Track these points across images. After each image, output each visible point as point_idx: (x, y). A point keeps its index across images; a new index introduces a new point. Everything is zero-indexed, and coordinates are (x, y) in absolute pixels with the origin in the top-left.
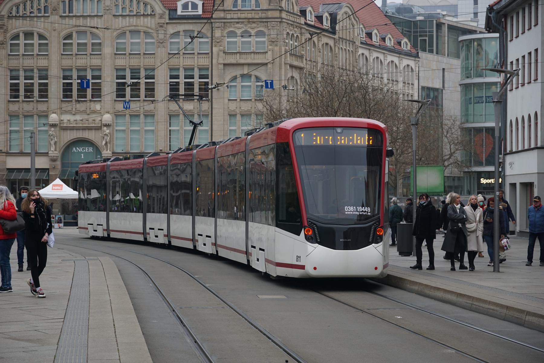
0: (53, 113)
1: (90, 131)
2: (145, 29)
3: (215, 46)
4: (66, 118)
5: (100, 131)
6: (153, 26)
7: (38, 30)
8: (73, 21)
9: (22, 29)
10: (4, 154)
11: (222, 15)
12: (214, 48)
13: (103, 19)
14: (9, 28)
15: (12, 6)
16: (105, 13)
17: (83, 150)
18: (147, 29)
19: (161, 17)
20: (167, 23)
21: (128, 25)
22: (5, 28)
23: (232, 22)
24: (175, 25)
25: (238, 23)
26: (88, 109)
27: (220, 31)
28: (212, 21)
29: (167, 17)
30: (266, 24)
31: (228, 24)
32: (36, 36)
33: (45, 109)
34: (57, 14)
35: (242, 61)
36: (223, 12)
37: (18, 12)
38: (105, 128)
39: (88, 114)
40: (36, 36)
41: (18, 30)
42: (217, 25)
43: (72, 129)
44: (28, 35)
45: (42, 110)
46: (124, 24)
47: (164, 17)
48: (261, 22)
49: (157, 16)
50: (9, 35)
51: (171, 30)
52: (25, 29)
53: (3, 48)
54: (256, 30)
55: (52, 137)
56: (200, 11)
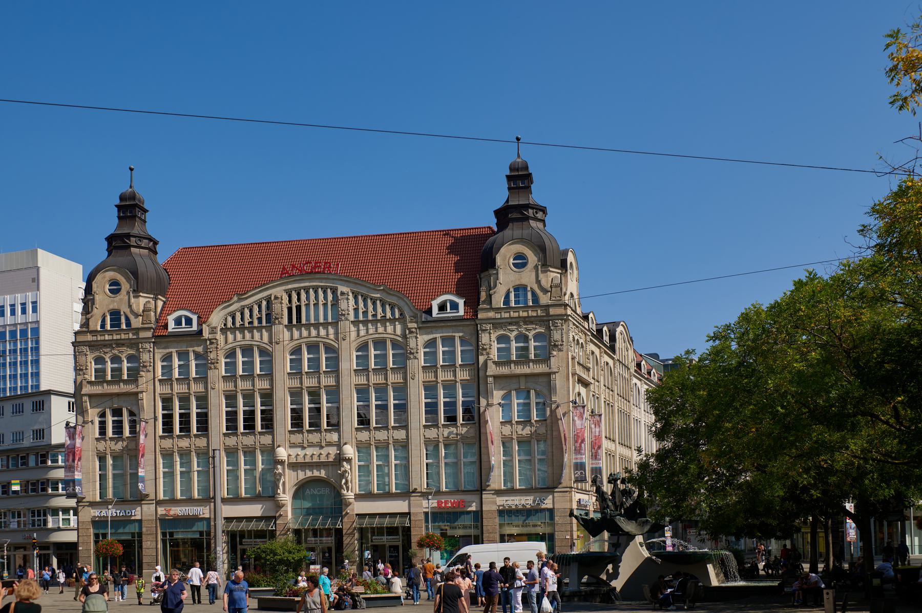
4: (294, 452)
11: (491, 314)
12: (480, 357)
56: (461, 312)
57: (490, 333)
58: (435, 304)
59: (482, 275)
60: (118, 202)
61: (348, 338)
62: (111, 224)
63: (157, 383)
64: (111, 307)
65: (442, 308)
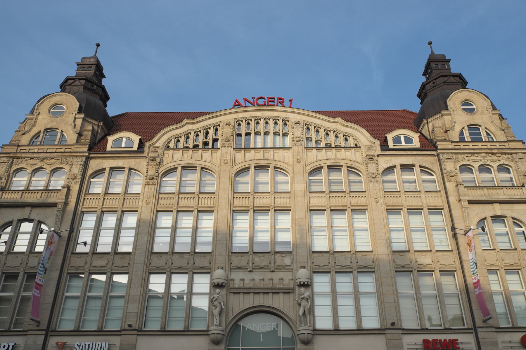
0: (218, 268)
1: (276, 296)
2: (349, 162)
3: (450, 181)
5: (291, 295)
6: (360, 160)
7: (203, 163)
8: (250, 155)
9: (182, 162)
10: (135, 332)
12: (447, 184)
13: (291, 151)
14: (164, 163)
15: (171, 137)
16: (295, 145)
18: (351, 163)
19: (369, 148)
20: (379, 155)
21: (325, 158)
23: (464, 154)
25: (473, 154)
26: (272, 262)
27: (452, 163)
29: (379, 148)
30: (510, 156)
31: (460, 157)
33: (206, 264)
35: (495, 197)
36: (450, 143)
38: (302, 289)
39: (273, 271)
41: (175, 163)
43: (247, 292)
45: (201, 265)
47: (374, 148)
48: (502, 154)
49: (364, 149)
50: (162, 170)
51: (384, 163)
54: (498, 164)
55: (216, 303)
57: (454, 162)
58: (390, 137)
59: (429, 120)
65: (397, 140)
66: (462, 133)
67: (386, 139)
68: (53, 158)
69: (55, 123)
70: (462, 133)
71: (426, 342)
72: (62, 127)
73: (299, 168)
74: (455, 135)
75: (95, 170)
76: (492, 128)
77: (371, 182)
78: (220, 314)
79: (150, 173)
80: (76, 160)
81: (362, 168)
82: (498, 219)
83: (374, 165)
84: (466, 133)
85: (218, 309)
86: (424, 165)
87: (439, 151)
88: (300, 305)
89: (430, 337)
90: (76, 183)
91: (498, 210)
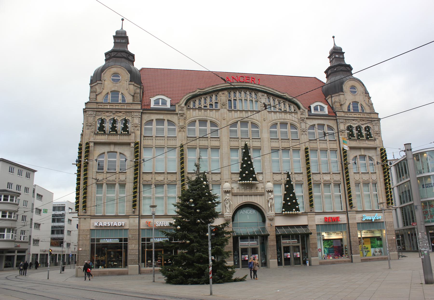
0: (226, 182)
2: (291, 121)
7: (211, 119)
14: (188, 117)
17: (248, 212)
20: (307, 118)
21: (278, 118)
22: (185, 116)
23: (349, 119)
24: (311, 120)
25: (354, 120)
28: (337, 118)
29: (307, 114)
31: (347, 121)
32: (208, 124)
34: (225, 108)
37: (194, 106)
38: (270, 194)
40: (208, 124)
41: (195, 118)
42: (341, 121)
44: (203, 122)
45: (216, 180)
46: (276, 118)
47: (304, 114)
48: (368, 120)
50: (187, 122)
51: (310, 122)
52: (201, 118)
53: (184, 131)
57: (344, 124)
58: (312, 106)
59: (333, 96)
60: (115, 34)
61: (266, 121)
62: (110, 46)
63: (142, 138)
64: (113, 89)
65: (316, 109)
66: (349, 107)
67: (310, 107)
68: (120, 112)
69: (116, 88)
70: (349, 107)
71: (326, 218)
72: (121, 91)
73: (264, 124)
74: (345, 108)
75: (147, 120)
76: (364, 105)
77: (302, 134)
78: (230, 206)
79: (181, 124)
80: (135, 114)
81: (298, 125)
82: (363, 157)
83: (304, 124)
84: (351, 107)
85: (228, 204)
86: (330, 124)
87: (337, 118)
88: (268, 201)
89: (328, 216)
90: (138, 130)
91: (363, 152)
